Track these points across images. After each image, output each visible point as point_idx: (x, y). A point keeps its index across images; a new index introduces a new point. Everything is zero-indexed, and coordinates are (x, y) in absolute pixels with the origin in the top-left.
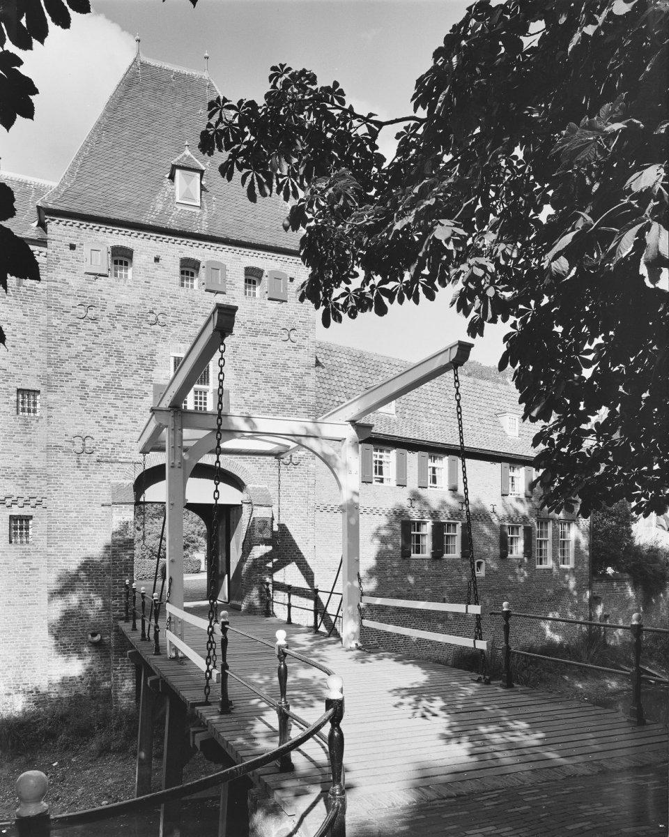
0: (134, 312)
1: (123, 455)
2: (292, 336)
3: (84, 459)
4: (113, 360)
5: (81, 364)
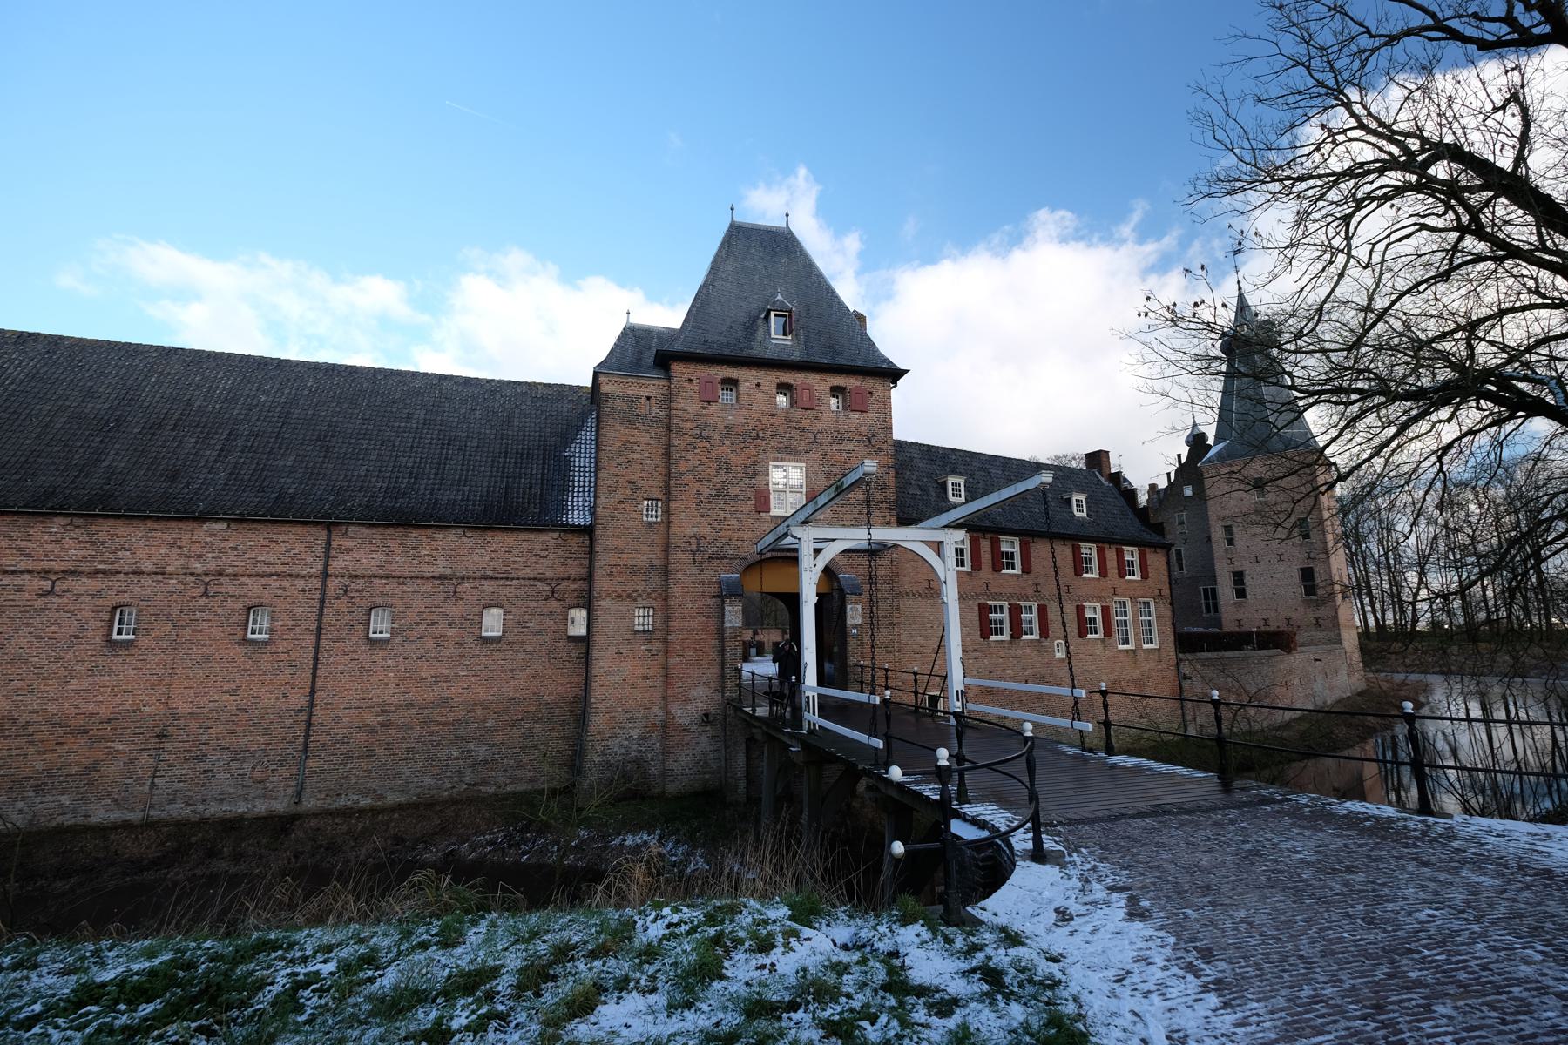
2: (873, 442)
4: (722, 472)
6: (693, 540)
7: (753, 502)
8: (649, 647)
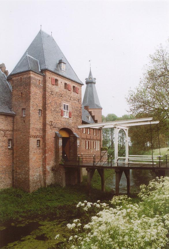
0: (58, 93)
1: (57, 126)
4: (55, 104)
7: (61, 113)
8: (40, 151)
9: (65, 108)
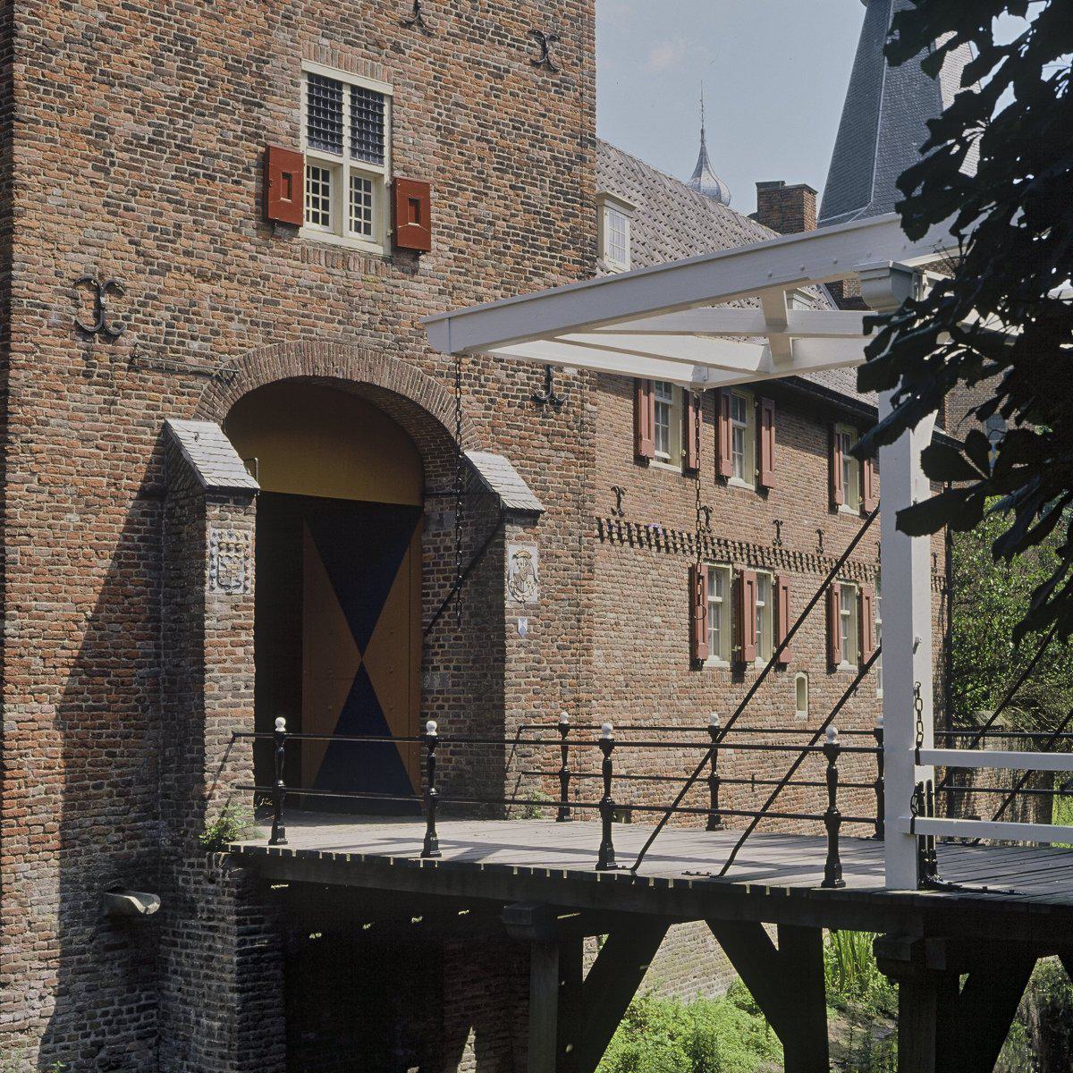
1: (195, 345)
3: (102, 349)
4: (172, 65)
5: (96, 63)
6: (85, 293)
9: (325, 131)
